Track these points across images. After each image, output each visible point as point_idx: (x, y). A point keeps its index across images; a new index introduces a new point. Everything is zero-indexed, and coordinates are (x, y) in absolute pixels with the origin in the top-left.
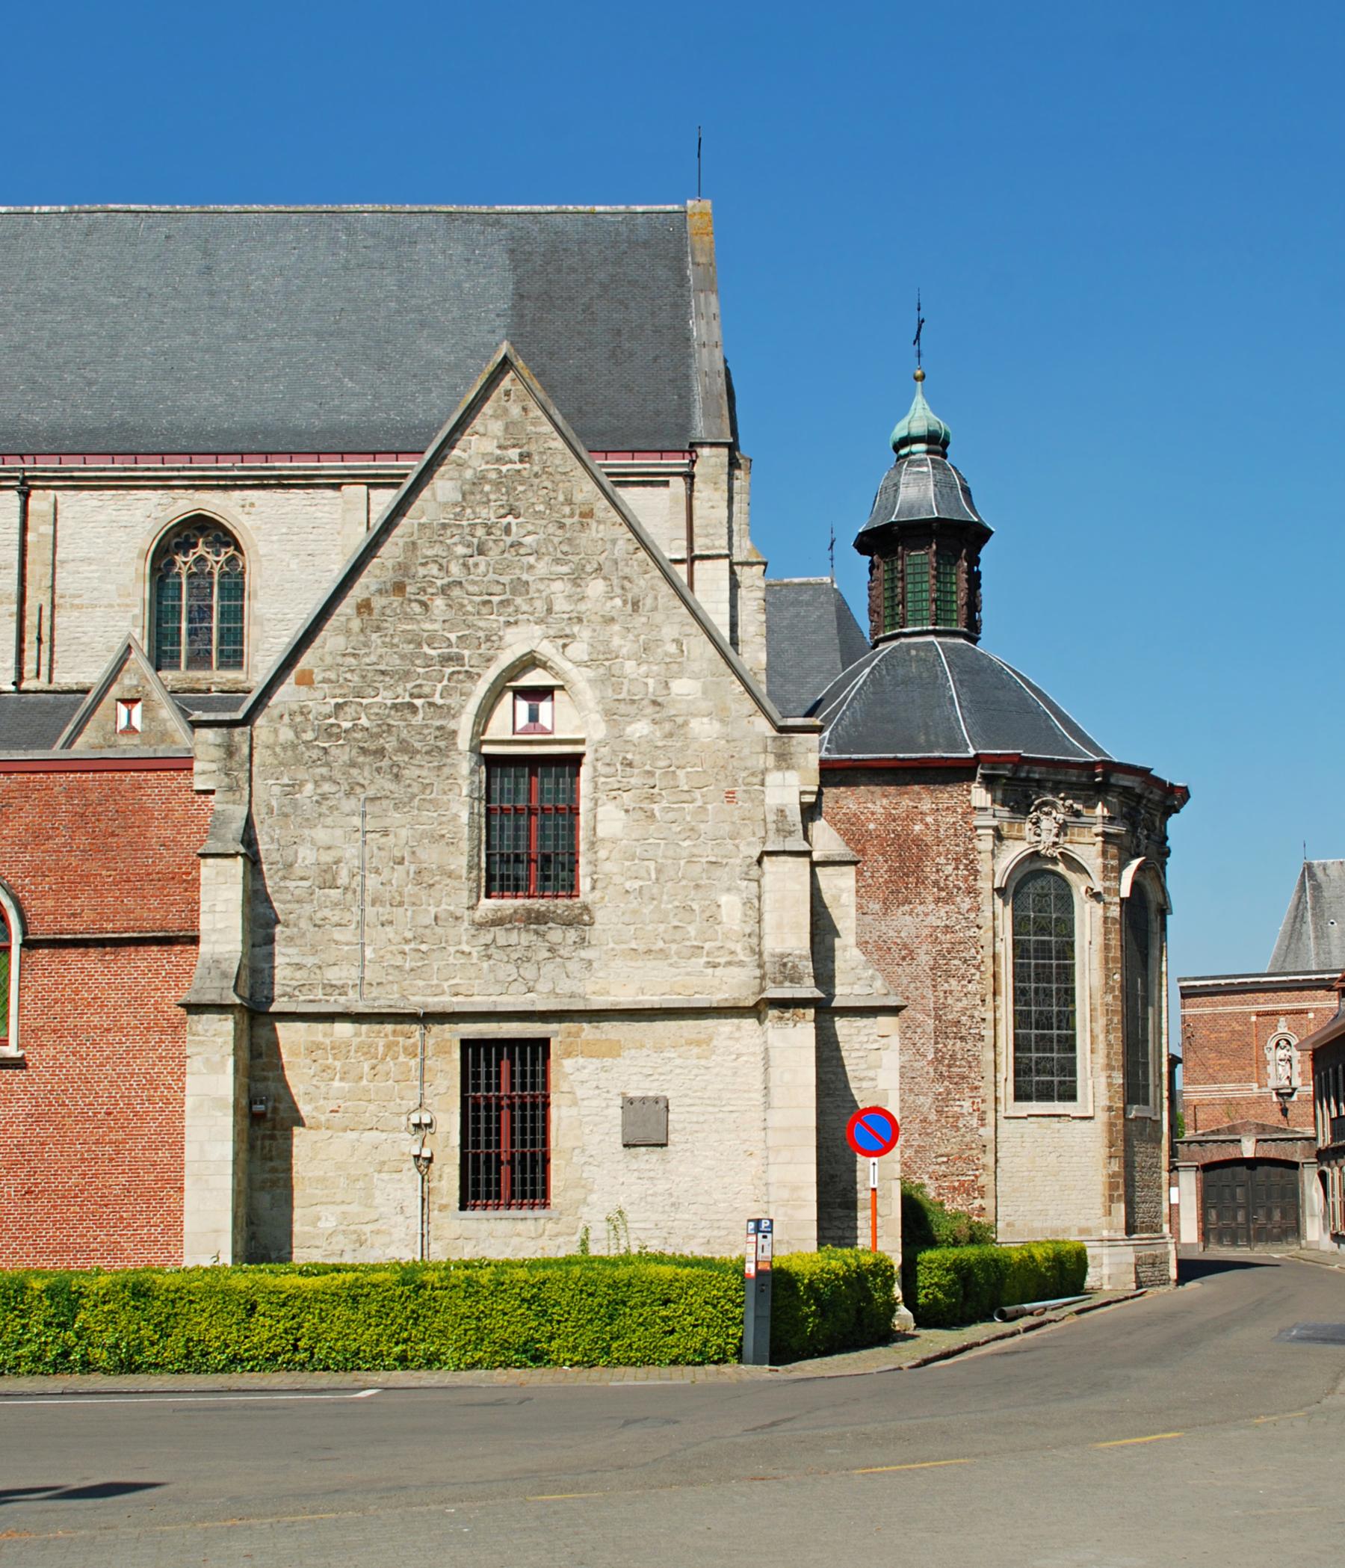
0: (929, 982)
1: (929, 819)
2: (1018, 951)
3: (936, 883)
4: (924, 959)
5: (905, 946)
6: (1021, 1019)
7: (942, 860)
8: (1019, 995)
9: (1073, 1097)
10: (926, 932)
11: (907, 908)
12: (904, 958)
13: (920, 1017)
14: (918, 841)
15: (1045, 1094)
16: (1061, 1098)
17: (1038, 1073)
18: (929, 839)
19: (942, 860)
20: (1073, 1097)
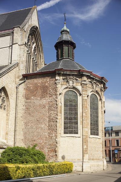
0: (48, 112)
1: (48, 82)
2: (65, 106)
3: (49, 94)
4: (47, 107)
5: (44, 105)
6: (65, 118)
7: (50, 89)
8: (65, 113)
9: (77, 133)
10: (48, 102)
11: (44, 98)
12: (43, 107)
13: (46, 118)
14: (47, 87)
15: (71, 132)
16: (74, 133)
17: (69, 128)
18: (48, 86)
19: (50, 89)
20: (77, 133)
